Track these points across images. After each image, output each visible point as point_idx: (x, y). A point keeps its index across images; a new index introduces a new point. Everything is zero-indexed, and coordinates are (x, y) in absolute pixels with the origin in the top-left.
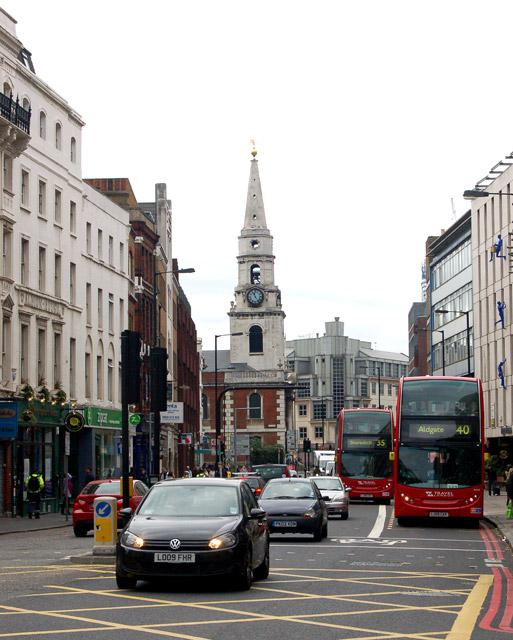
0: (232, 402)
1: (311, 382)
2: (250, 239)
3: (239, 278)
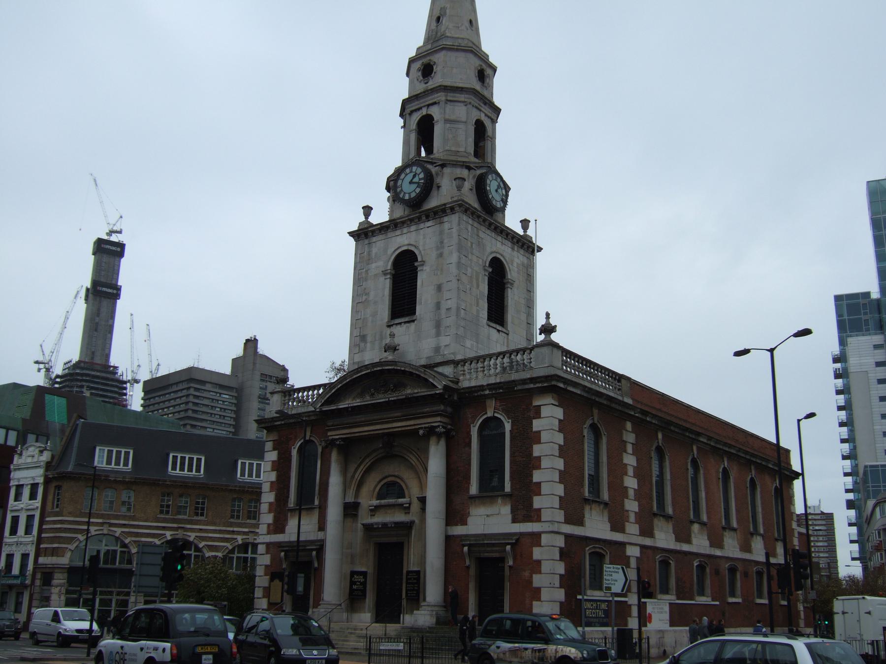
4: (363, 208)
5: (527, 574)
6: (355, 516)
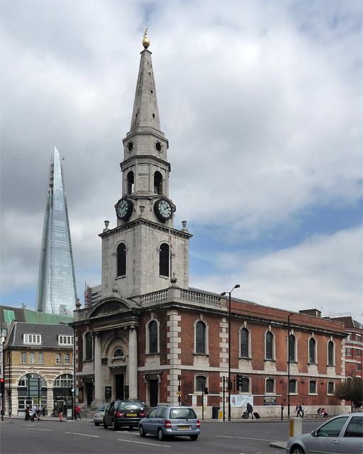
5: (165, 386)
6: (106, 364)
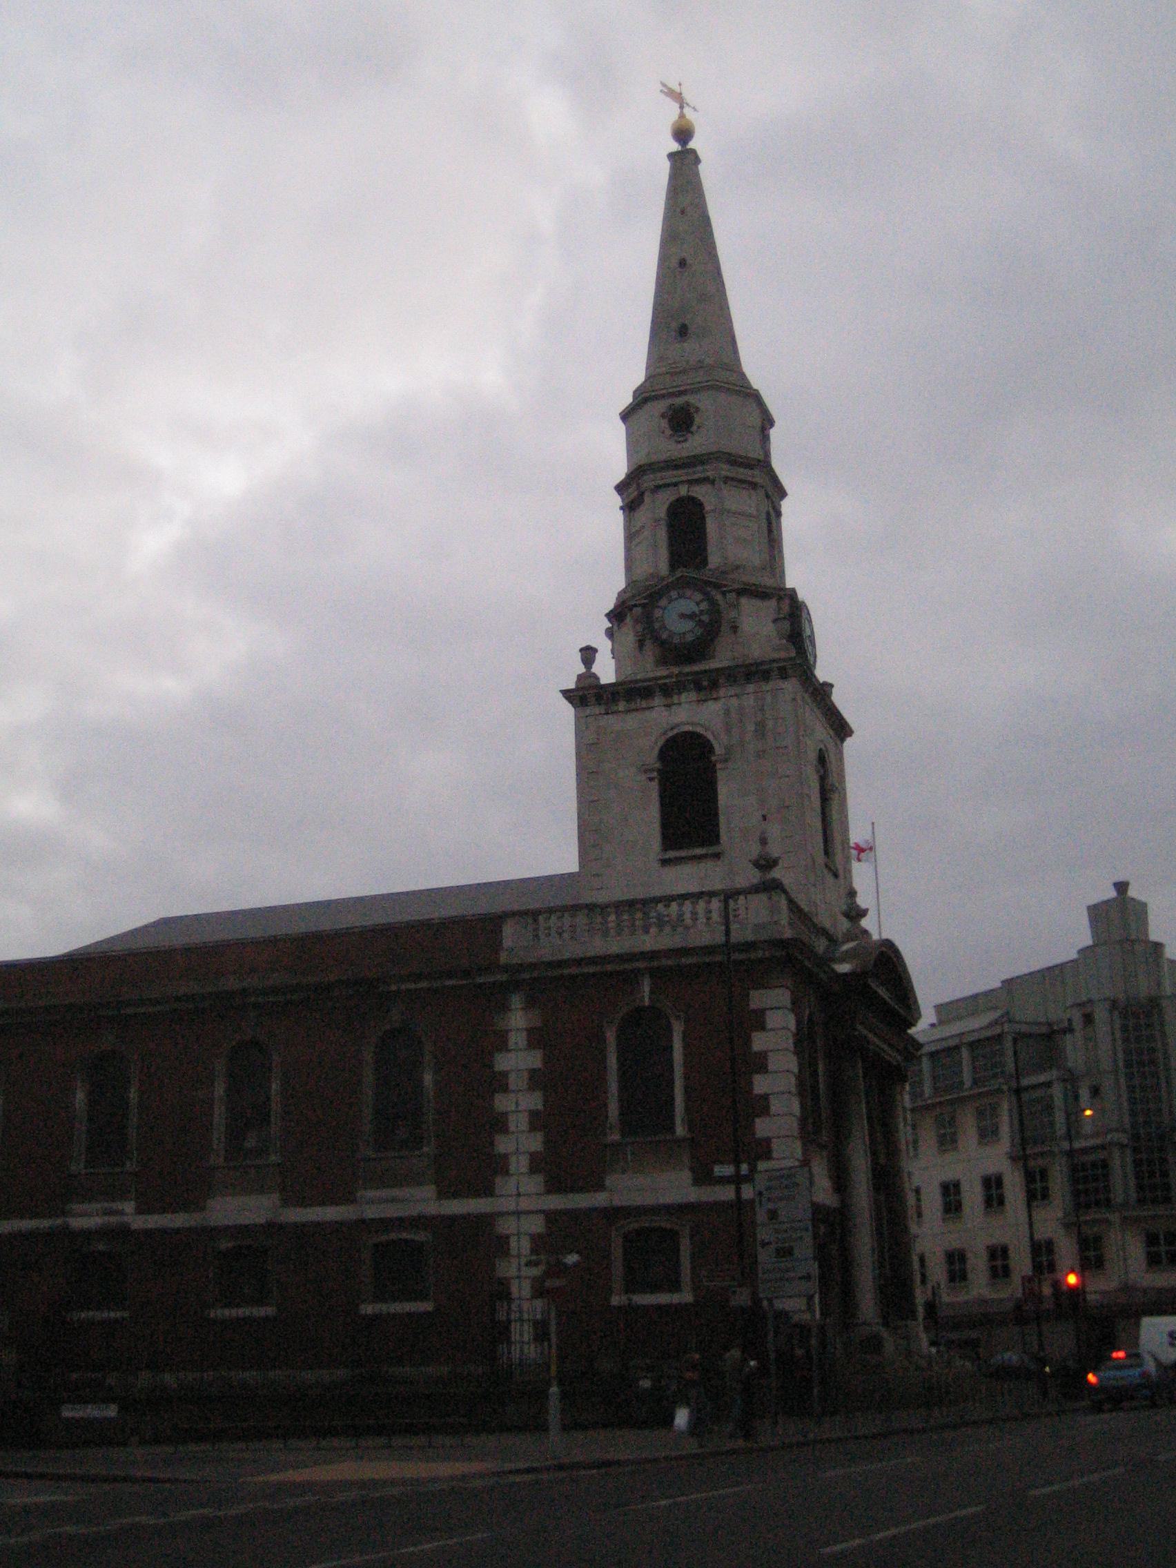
0: (534, 1059)
1: (1057, 1092)
2: (661, 406)
3: (629, 568)
4: (581, 650)
